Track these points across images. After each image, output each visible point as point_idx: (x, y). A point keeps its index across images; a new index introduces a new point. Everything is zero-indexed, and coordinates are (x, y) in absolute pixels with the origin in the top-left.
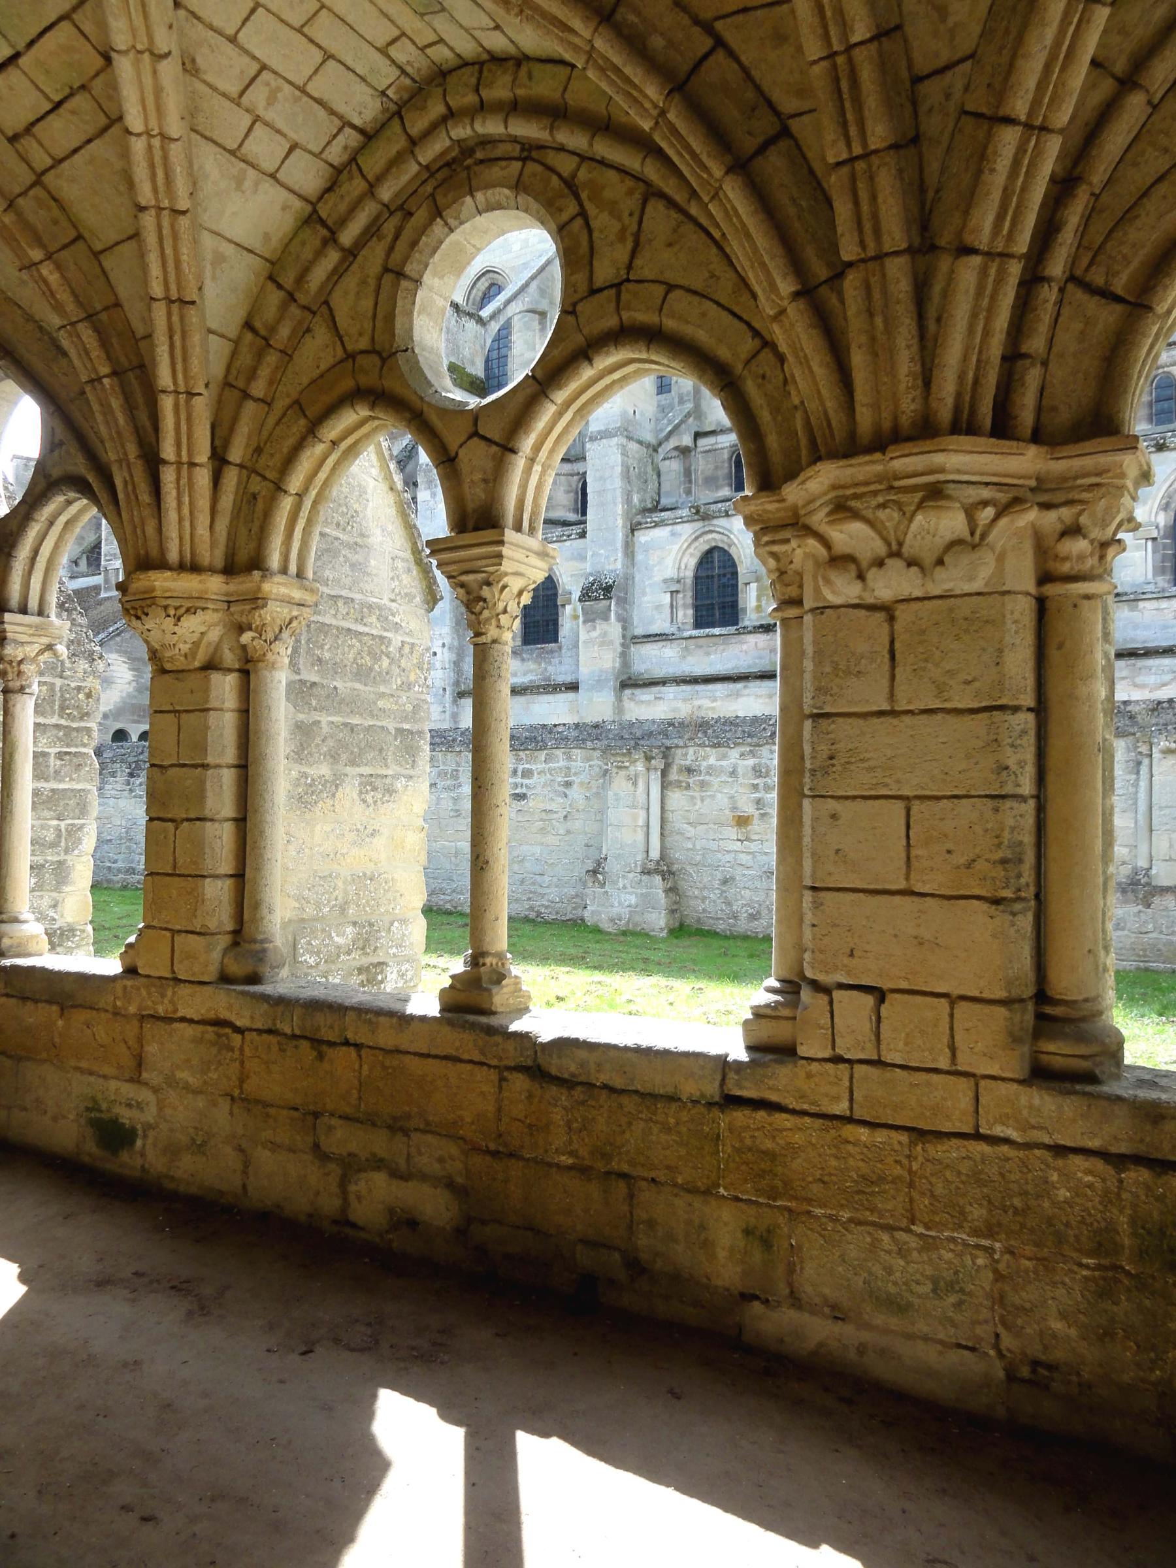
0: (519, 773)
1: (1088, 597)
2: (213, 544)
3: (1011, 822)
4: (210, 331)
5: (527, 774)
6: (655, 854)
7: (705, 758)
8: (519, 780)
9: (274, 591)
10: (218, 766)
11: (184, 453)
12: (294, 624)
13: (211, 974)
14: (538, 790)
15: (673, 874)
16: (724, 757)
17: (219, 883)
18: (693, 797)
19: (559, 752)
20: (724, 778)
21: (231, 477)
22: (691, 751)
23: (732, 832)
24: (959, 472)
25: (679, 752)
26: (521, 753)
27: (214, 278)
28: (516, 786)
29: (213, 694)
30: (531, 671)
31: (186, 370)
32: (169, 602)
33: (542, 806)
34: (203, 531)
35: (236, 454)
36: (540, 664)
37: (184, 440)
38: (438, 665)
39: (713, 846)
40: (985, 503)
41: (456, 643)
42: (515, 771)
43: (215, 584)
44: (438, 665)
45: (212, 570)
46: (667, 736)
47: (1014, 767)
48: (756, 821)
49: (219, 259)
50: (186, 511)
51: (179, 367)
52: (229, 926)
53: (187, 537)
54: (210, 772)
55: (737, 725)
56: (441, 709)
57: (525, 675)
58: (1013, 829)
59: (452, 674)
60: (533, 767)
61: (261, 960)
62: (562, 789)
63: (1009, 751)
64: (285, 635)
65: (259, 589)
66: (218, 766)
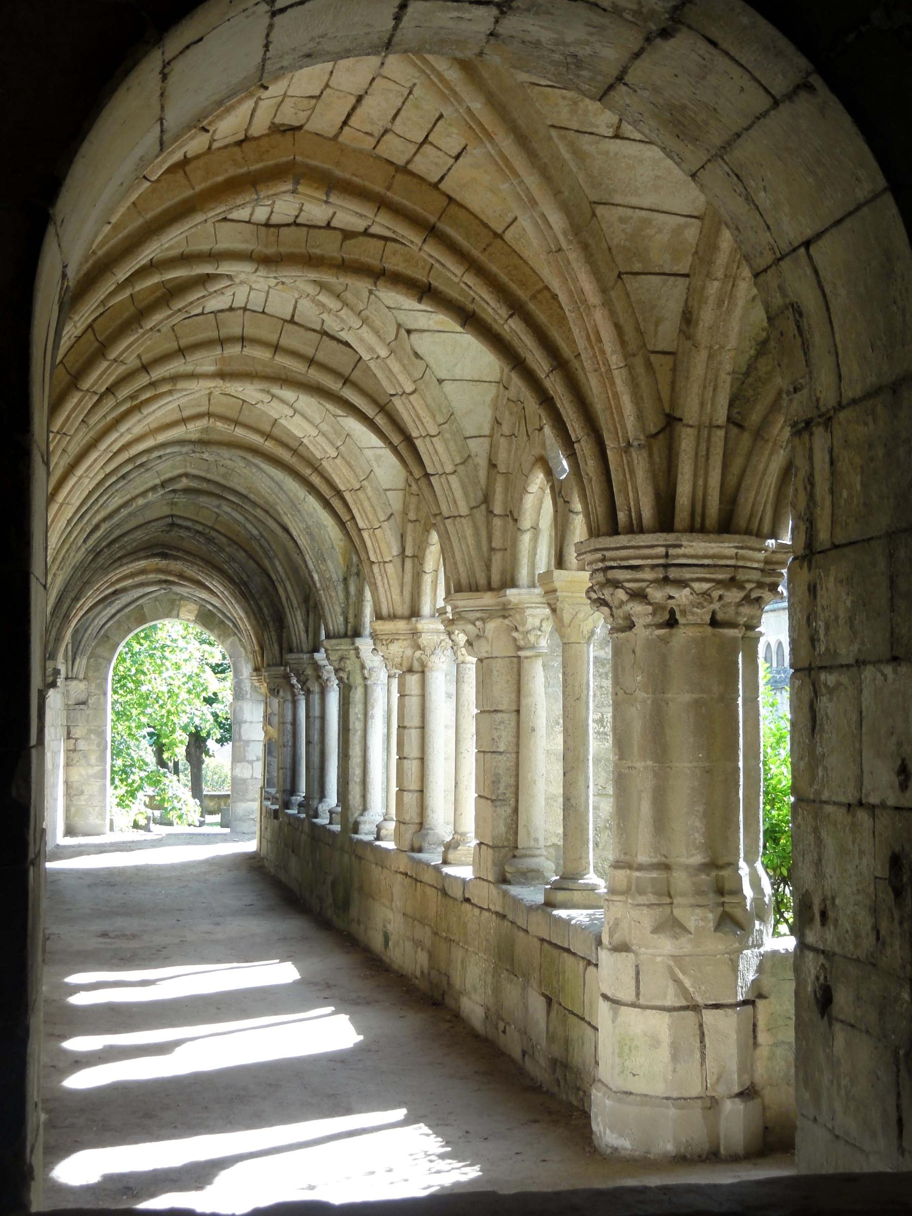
1: (527, 658)
2: (403, 602)
3: (495, 764)
4: (387, 490)
9: (426, 627)
10: (410, 728)
11: (379, 557)
12: (443, 644)
13: (406, 846)
17: (410, 794)
21: (409, 563)
24: (464, 607)
27: (379, 466)
29: (407, 687)
31: (368, 519)
32: (383, 637)
34: (396, 597)
35: (409, 552)
37: (378, 551)
40: (478, 619)
43: (401, 625)
45: (402, 618)
47: (496, 739)
49: (378, 458)
50: (386, 586)
51: (364, 517)
52: (417, 821)
53: (390, 600)
54: (406, 731)
58: (496, 767)
61: (424, 840)
63: (494, 731)
64: (438, 651)
65: (416, 628)
66: (410, 728)
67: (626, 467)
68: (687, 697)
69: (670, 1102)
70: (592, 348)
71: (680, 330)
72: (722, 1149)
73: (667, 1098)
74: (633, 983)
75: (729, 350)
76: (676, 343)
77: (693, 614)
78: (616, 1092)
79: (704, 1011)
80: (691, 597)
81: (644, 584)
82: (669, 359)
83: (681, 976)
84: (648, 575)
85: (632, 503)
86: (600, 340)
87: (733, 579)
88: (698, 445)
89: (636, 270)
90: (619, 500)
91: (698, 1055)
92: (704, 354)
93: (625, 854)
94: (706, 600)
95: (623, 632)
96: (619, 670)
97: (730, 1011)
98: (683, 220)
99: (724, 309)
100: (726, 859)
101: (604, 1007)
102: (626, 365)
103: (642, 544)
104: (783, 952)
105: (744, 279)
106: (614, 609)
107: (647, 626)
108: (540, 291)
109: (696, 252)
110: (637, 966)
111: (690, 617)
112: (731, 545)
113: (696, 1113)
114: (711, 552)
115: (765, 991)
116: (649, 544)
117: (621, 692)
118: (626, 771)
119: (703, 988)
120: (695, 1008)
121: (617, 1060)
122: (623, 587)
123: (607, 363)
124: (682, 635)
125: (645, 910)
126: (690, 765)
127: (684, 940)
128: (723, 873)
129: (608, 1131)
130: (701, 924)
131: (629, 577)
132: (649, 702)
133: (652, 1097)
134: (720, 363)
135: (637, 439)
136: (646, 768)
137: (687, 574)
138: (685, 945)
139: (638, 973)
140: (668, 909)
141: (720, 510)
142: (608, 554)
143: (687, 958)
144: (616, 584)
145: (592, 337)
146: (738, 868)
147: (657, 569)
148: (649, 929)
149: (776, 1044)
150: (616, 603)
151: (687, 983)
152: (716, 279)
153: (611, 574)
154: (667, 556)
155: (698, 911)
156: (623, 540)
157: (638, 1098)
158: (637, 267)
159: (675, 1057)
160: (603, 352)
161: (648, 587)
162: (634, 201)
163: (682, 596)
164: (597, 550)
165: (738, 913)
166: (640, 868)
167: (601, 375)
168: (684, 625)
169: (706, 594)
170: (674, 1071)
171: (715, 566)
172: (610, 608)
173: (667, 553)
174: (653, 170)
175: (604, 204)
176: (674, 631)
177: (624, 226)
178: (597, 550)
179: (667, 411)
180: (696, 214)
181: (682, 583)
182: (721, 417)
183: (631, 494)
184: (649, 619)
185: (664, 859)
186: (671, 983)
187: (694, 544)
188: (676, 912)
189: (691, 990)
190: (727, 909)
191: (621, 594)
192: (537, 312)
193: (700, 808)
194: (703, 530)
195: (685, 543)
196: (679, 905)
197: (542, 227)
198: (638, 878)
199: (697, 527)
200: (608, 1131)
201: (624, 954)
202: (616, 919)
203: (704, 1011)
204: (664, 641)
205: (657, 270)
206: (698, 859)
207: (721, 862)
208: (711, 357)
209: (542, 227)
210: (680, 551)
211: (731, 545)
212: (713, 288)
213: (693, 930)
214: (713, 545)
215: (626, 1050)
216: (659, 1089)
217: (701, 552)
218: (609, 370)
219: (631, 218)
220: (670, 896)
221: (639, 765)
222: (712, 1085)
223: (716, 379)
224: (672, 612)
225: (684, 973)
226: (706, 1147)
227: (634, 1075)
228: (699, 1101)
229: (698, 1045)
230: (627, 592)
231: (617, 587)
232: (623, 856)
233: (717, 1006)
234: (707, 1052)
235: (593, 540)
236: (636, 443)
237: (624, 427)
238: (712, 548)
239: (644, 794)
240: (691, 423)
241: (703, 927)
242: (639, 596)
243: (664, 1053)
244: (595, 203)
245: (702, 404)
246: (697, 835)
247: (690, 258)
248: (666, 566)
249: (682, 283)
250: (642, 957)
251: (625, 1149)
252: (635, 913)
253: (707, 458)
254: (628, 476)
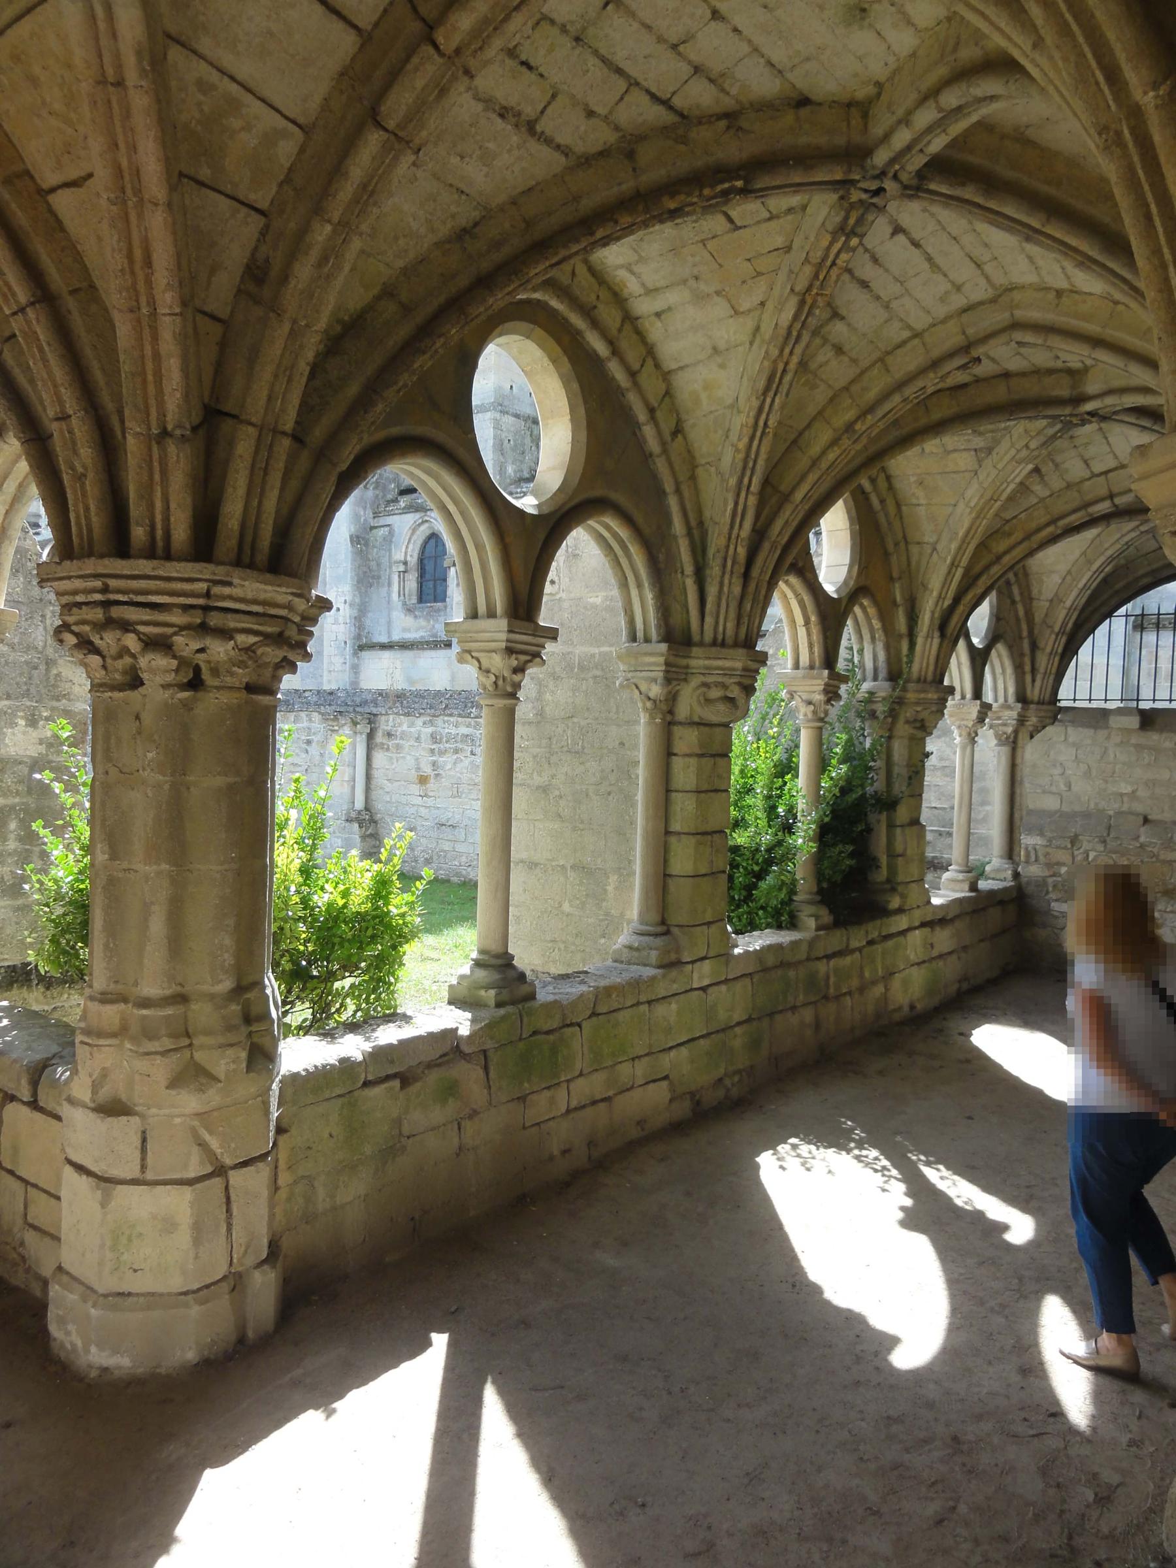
6: (359, 804)
7: (400, 725)
15: (376, 822)
16: (412, 725)
18: (391, 758)
19: (303, 714)
20: (412, 742)
22: (391, 717)
23: (415, 789)
25: (383, 718)
30: (422, 628)
38: (341, 620)
39: (403, 799)
41: (357, 600)
44: (341, 620)
46: (376, 705)
48: (432, 780)
55: (424, 698)
56: (342, 660)
59: (353, 629)
62: (305, 746)
67: (156, 464)
68: (220, 781)
69: (190, 1297)
70: (133, 273)
71: (239, 291)
72: (250, 1334)
73: (185, 1293)
74: (138, 1154)
75: (316, 332)
76: (229, 308)
77: (232, 674)
78: (106, 1296)
79: (231, 1173)
80: (232, 653)
81: (170, 630)
82: (217, 330)
83: (207, 1137)
84: (177, 618)
85: (159, 518)
86: (148, 263)
87: (281, 634)
88: (257, 452)
89: (201, 178)
90: (136, 510)
91: (224, 1229)
92: (287, 327)
93: (116, 982)
94: (250, 658)
95: (120, 690)
96: (113, 741)
97: (261, 1165)
98: (284, 123)
99: (326, 270)
100: (251, 979)
101: (74, 1185)
102: (181, 314)
103: (175, 575)
104: (304, 1073)
105: (361, 234)
106: (109, 661)
107: (165, 687)
108: (18, 176)
109: (287, 180)
110: (144, 1132)
111: (228, 679)
112: (289, 591)
113: (223, 1303)
114: (262, 596)
115: (284, 1125)
116: (186, 576)
117: (113, 772)
118: (120, 875)
119: (233, 1145)
120: (220, 1171)
121: (109, 1255)
122: (135, 631)
123: (152, 303)
124: (213, 702)
125: (158, 1060)
126: (220, 868)
127: (211, 1092)
128: (248, 996)
129: (93, 1349)
130: (233, 1066)
131: (146, 618)
132: (167, 787)
133: (161, 1295)
134: (302, 347)
135: (179, 426)
136: (159, 873)
137: (232, 622)
138: (213, 1097)
139: (144, 1140)
140: (187, 1054)
141: (272, 543)
142: (113, 583)
143: (215, 1114)
144: (126, 626)
145: (138, 253)
146: (264, 987)
147: (193, 611)
148: (164, 1083)
149: (295, 1182)
150: (114, 651)
151: (214, 1144)
152: (329, 221)
153: (116, 612)
154: (208, 595)
155: (230, 1052)
156: (144, 566)
157: (142, 1299)
158: (205, 173)
159: (197, 1241)
160: (149, 283)
161: (175, 634)
162: (228, 60)
163: (220, 650)
164: (96, 576)
165: (265, 1041)
166: (145, 1003)
167: (139, 321)
168: (217, 688)
169: (249, 650)
170: (196, 1257)
171: (264, 615)
172: (103, 657)
173: (208, 591)
174: (269, 17)
175: (183, 45)
176: (200, 694)
177: (202, 98)
178: (96, 576)
179: (206, 401)
180: (301, 120)
181: (225, 634)
182: (289, 423)
183: (158, 505)
184: (170, 678)
185: (179, 989)
186: (195, 1150)
187: (247, 583)
188: (199, 1056)
189: (218, 1151)
190: (255, 1040)
191: (131, 641)
192: (13, 206)
193: (231, 922)
194: (252, 566)
195: (236, 581)
196: (202, 1047)
197: (102, 25)
198: (144, 1017)
199: (244, 561)
200: (93, 1349)
201: (124, 1119)
202: (104, 1069)
203: (231, 1173)
204: (187, 706)
205: (229, 189)
206: (226, 985)
207: (244, 983)
208: (293, 334)
209: (102, 25)
210: (227, 590)
211: (289, 591)
212: (322, 233)
213: (222, 1077)
214: (269, 588)
215: (124, 1240)
216: (176, 1283)
217: (250, 596)
218: (154, 314)
219: (213, 87)
220: (188, 1035)
221: (150, 869)
222: (239, 1260)
223: (293, 367)
224: (197, 670)
225: (211, 1133)
226: (233, 1338)
227: (135, 1271)
228: (224, 1284)
229: (224, 1216)
230: (140, 639)
231: (127, 631)
232: (112, 986)
233: (245, 1164)
234: (234, 1222)
235: (67, 563)
236: (178, 432)
237: (161, 404)
238: (266, 591)
239: (155, 908)
240: (254, 420)
241: (234, 1070)
242: (153, 644)
243: (183, 1238)
244: (169, 36)
245: (270, 398)
246: (226, 956)
247: (274, 189)
248: (206, 609)
249: (257, 222)
250: (151, 1120)
251: (120, 1368)
252: (141, 1065)
253: (266, 471)
254: (157, 477)
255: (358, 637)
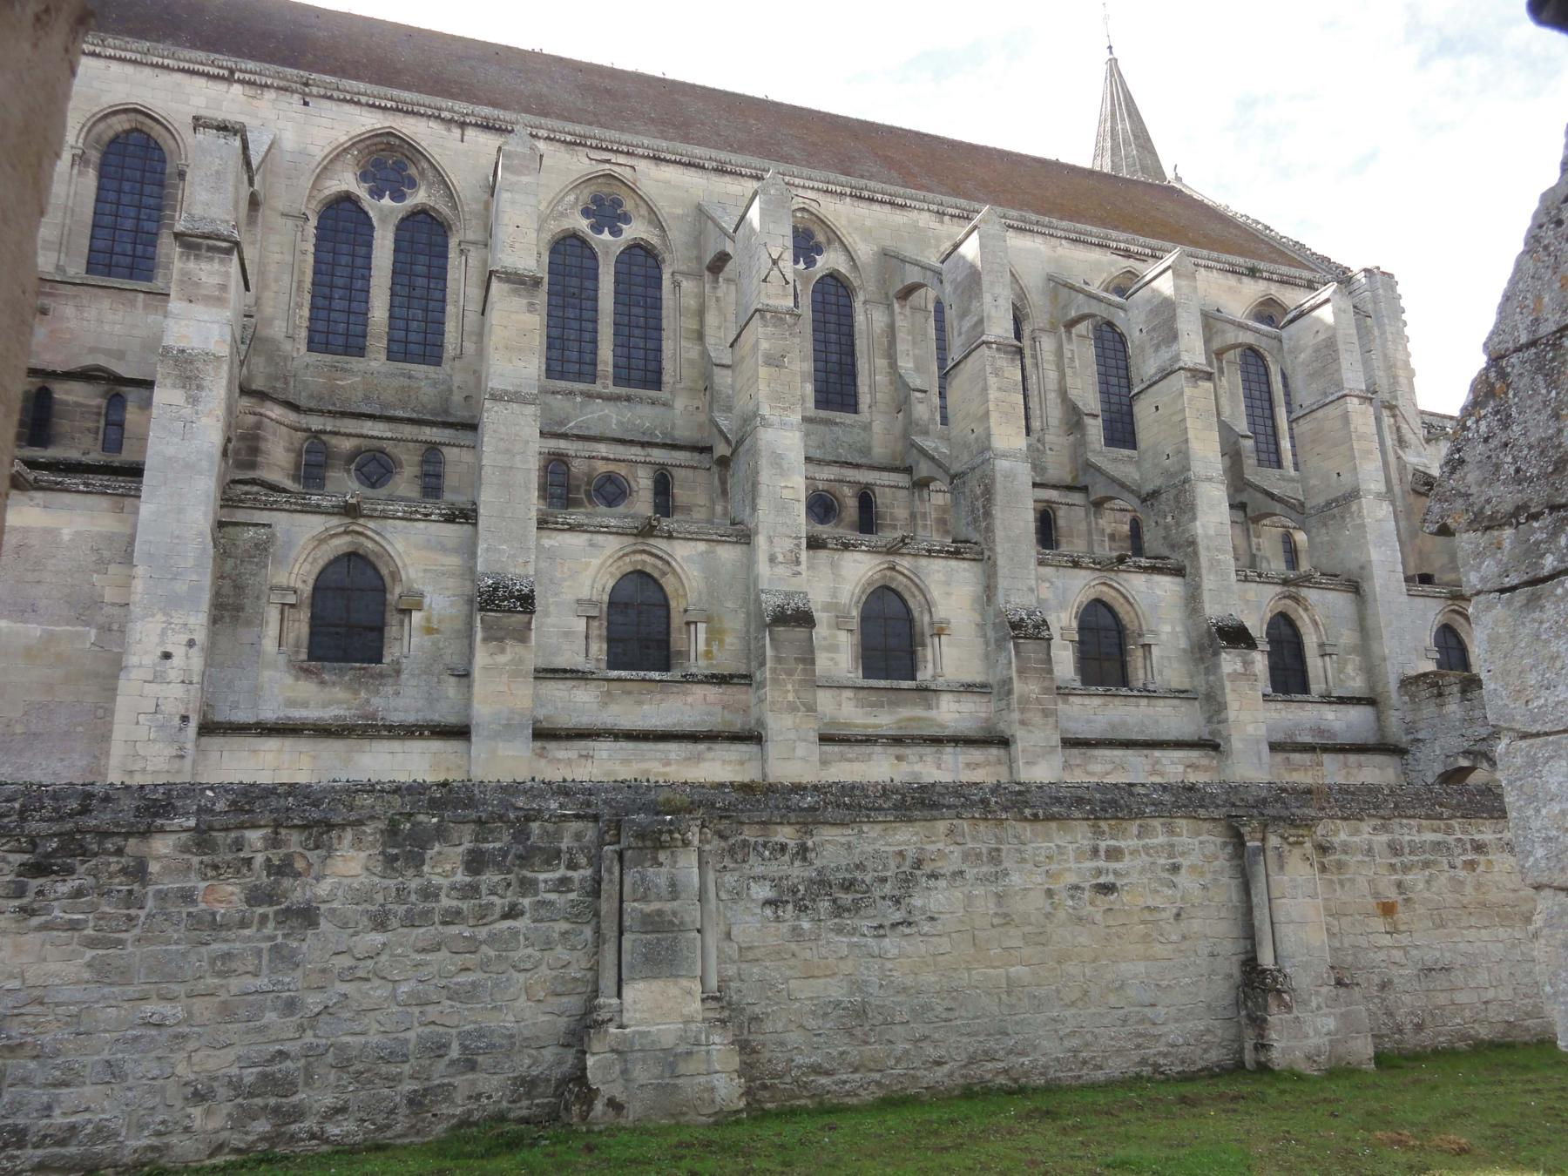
0: (1102, 853)
5: (1114, 854)
7: (1336, 833)
8: (1101, 864)
14: (1134, 878)
16: (1357, 832)
18: (1331, 881)
19: (1156, 823)
20: (1360, 857)
23: (1379, 924)
26: (1102, 824)
28: (1099, 872)
30: (339, 702)
33: (1141, 902)
36: (356, 693)
39: (1363, 942)
42: (1095, 851)
44: (173, 675)
48: (1400, 908)
57: (325, 705)
60: (1122, 844)
62: (1166, 875)
255: (207, 706)
